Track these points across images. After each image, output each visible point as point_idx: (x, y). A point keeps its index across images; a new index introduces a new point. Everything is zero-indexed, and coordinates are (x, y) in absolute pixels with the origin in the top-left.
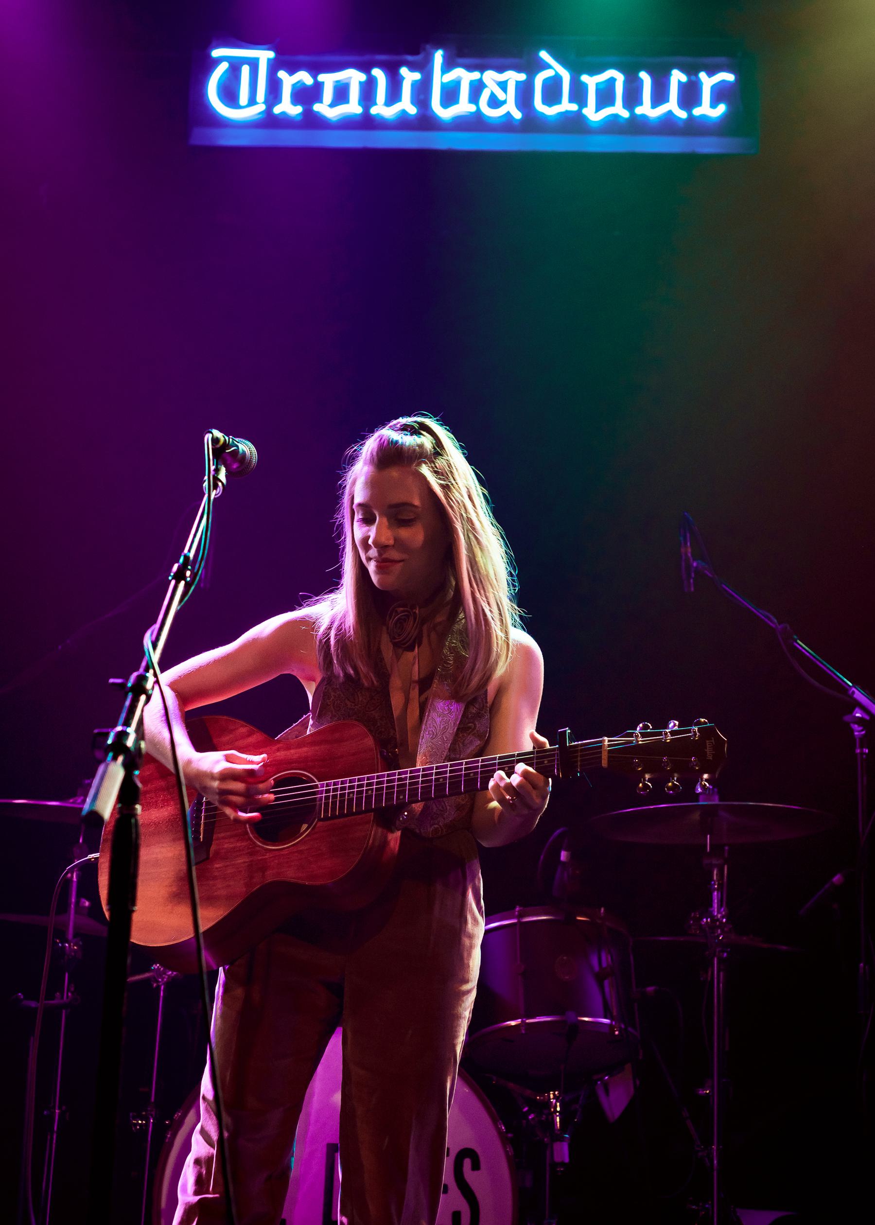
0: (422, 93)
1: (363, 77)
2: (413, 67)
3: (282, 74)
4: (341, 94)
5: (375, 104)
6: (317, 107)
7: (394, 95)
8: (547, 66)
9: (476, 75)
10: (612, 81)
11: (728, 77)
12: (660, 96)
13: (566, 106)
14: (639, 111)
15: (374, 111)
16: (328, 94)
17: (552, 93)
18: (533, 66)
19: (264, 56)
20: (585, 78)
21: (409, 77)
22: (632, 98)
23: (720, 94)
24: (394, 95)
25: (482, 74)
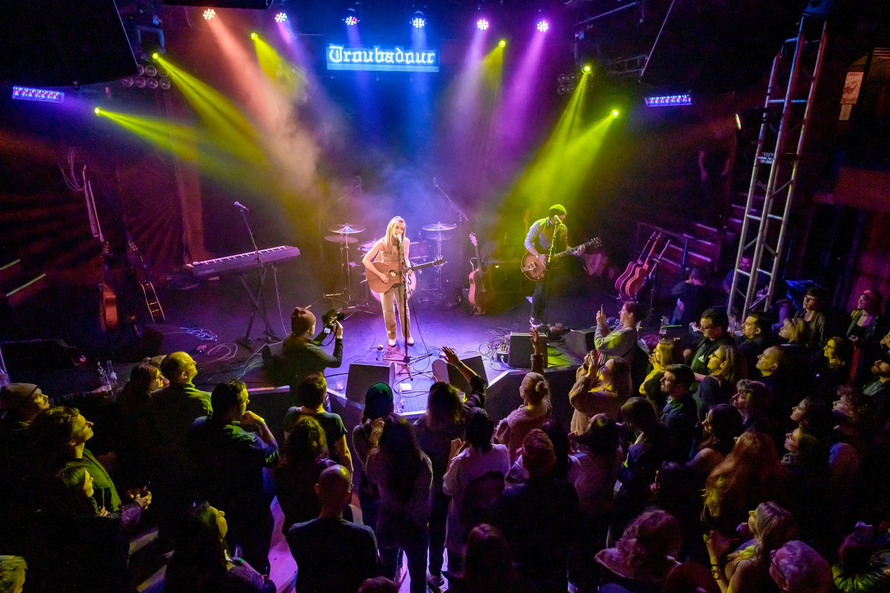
0: (374, 57)
1: (362, 53)
3: (345, 52)
4: (357, 56)
6: (353, 60)
7: (368, 57)
9: (384, 53)
11: (433, 54)
12: (420, 58)
13: (402, 60)
14: (416, 61)
15: (364, 61)
17: (399, 57)
18: (395, 52)
20: (406, 54)
21: (371, 53)
22: (415, 59)
23: (432, 58)
24: (368, 57)
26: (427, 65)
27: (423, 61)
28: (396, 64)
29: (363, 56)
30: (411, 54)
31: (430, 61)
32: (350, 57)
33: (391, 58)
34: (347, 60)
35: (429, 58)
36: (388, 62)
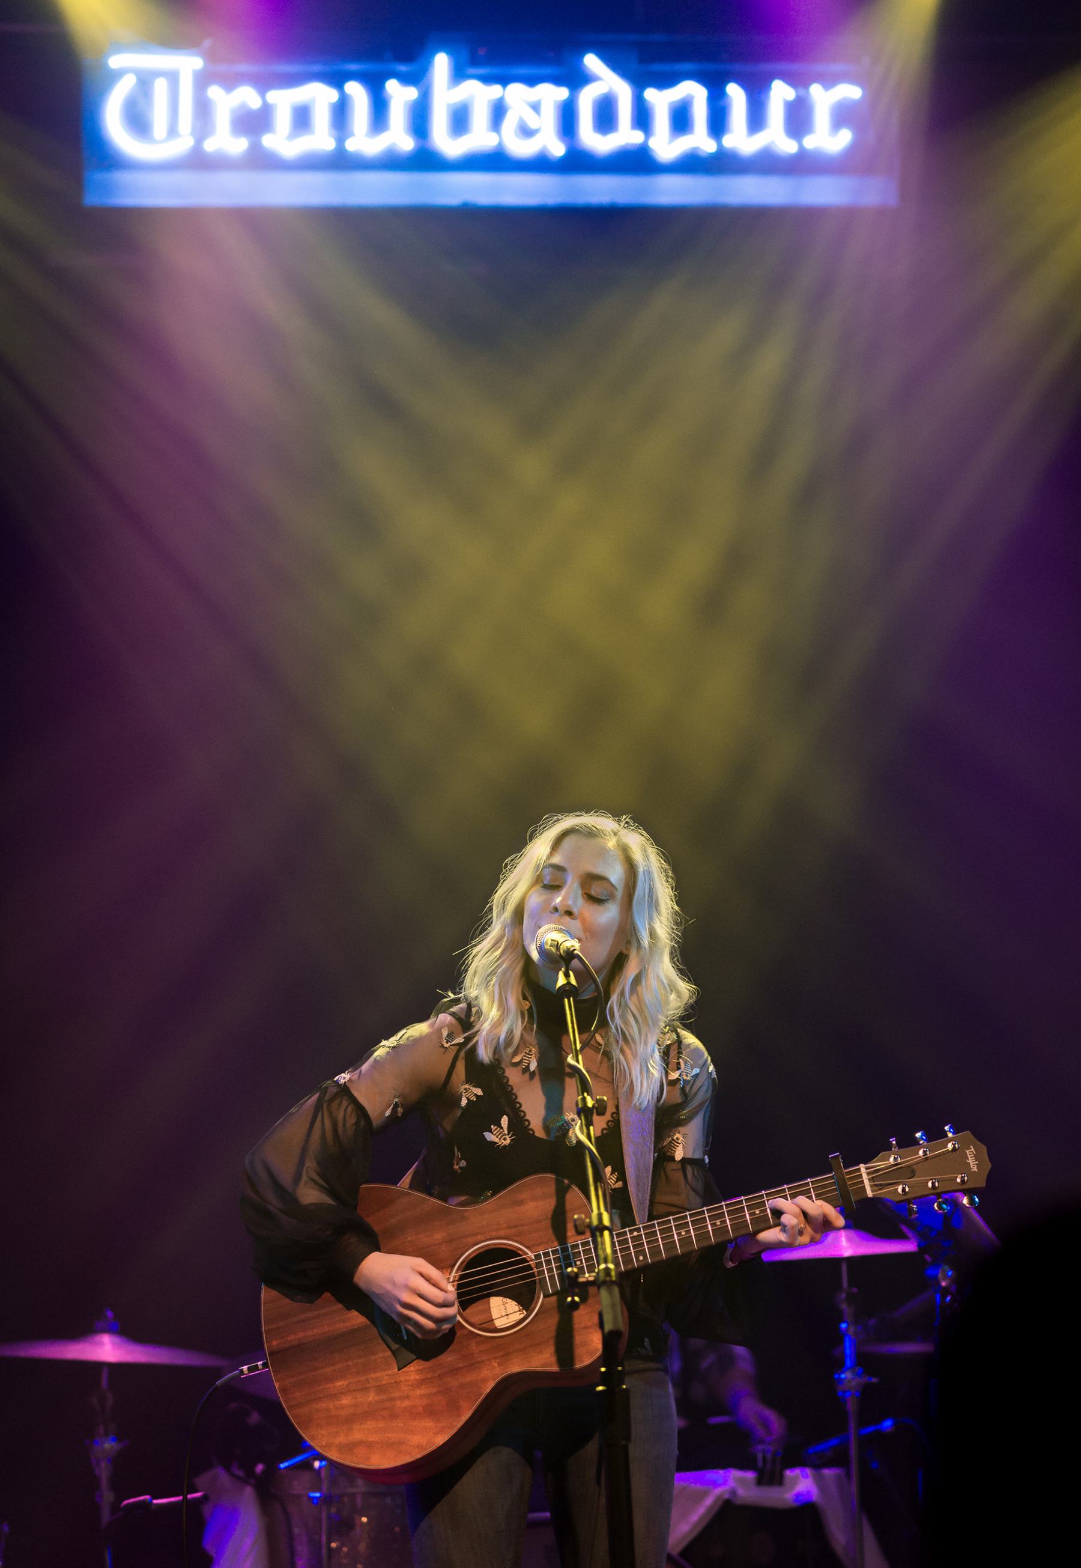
2: (407, 79)
5: (351, 134)
6: (270, 141)
16: (283, 119)
25: (504, 89)
29: (341, 112)
34: (232, 144)
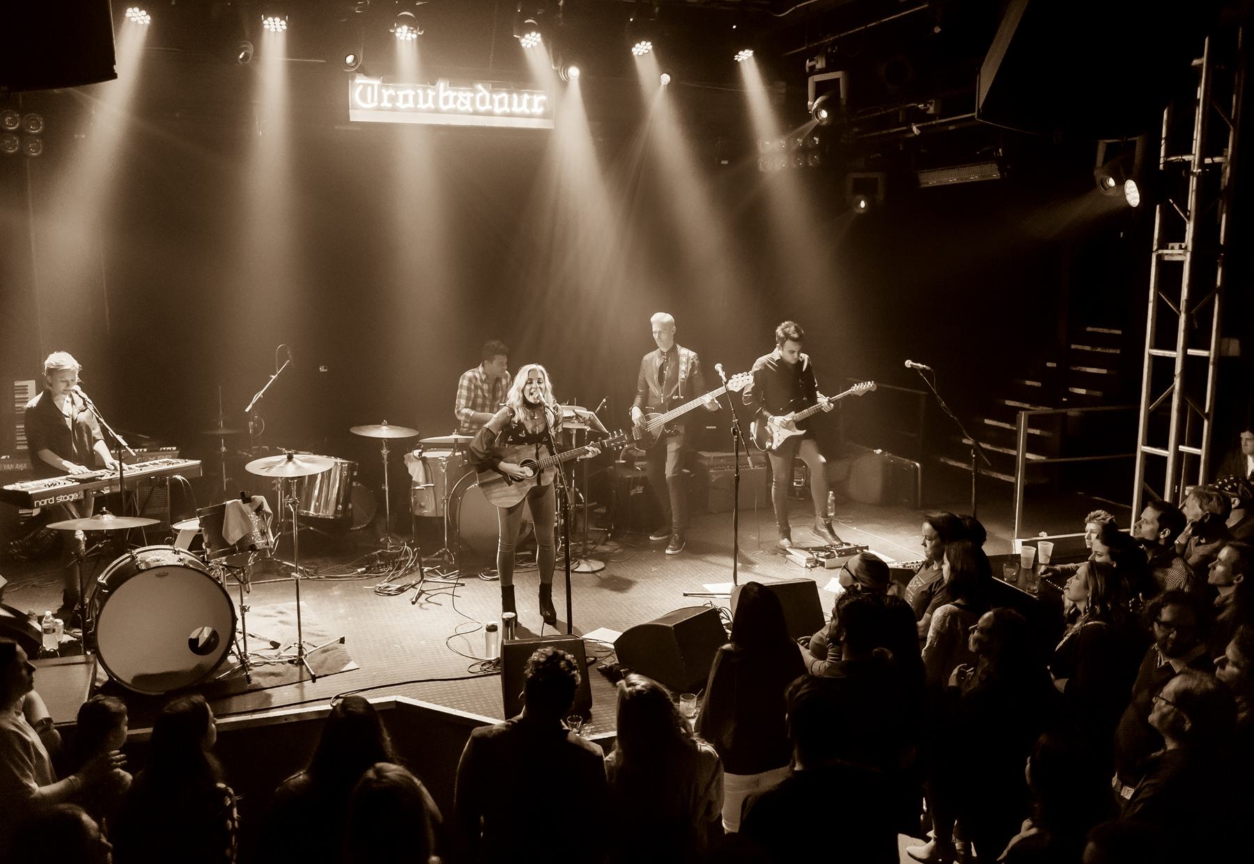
3: (384, 91)
4: (406, 98)
6: (397, 104)
7: (426, 101)
8: (481, 91)
9: (455, 94)
10: (503, 98)
11: (543, 98)
13: (487, 107)
15: (419, 106)
16: (401, 99)
17: (483, 102)
18: (475, 91)
19: (376, 82)
21: (431, 93)
23: (542, 104)
24: (426, 101)
26: (530, 116)
27: (524, 109)
28: (476, 113)
29: (416, 98)
30: (504, 95)
31: (538, 110)
32: (393, 99)
33: (468, 102)
34: (386, 104)
35: (536, 104)
36: (462, 109)
